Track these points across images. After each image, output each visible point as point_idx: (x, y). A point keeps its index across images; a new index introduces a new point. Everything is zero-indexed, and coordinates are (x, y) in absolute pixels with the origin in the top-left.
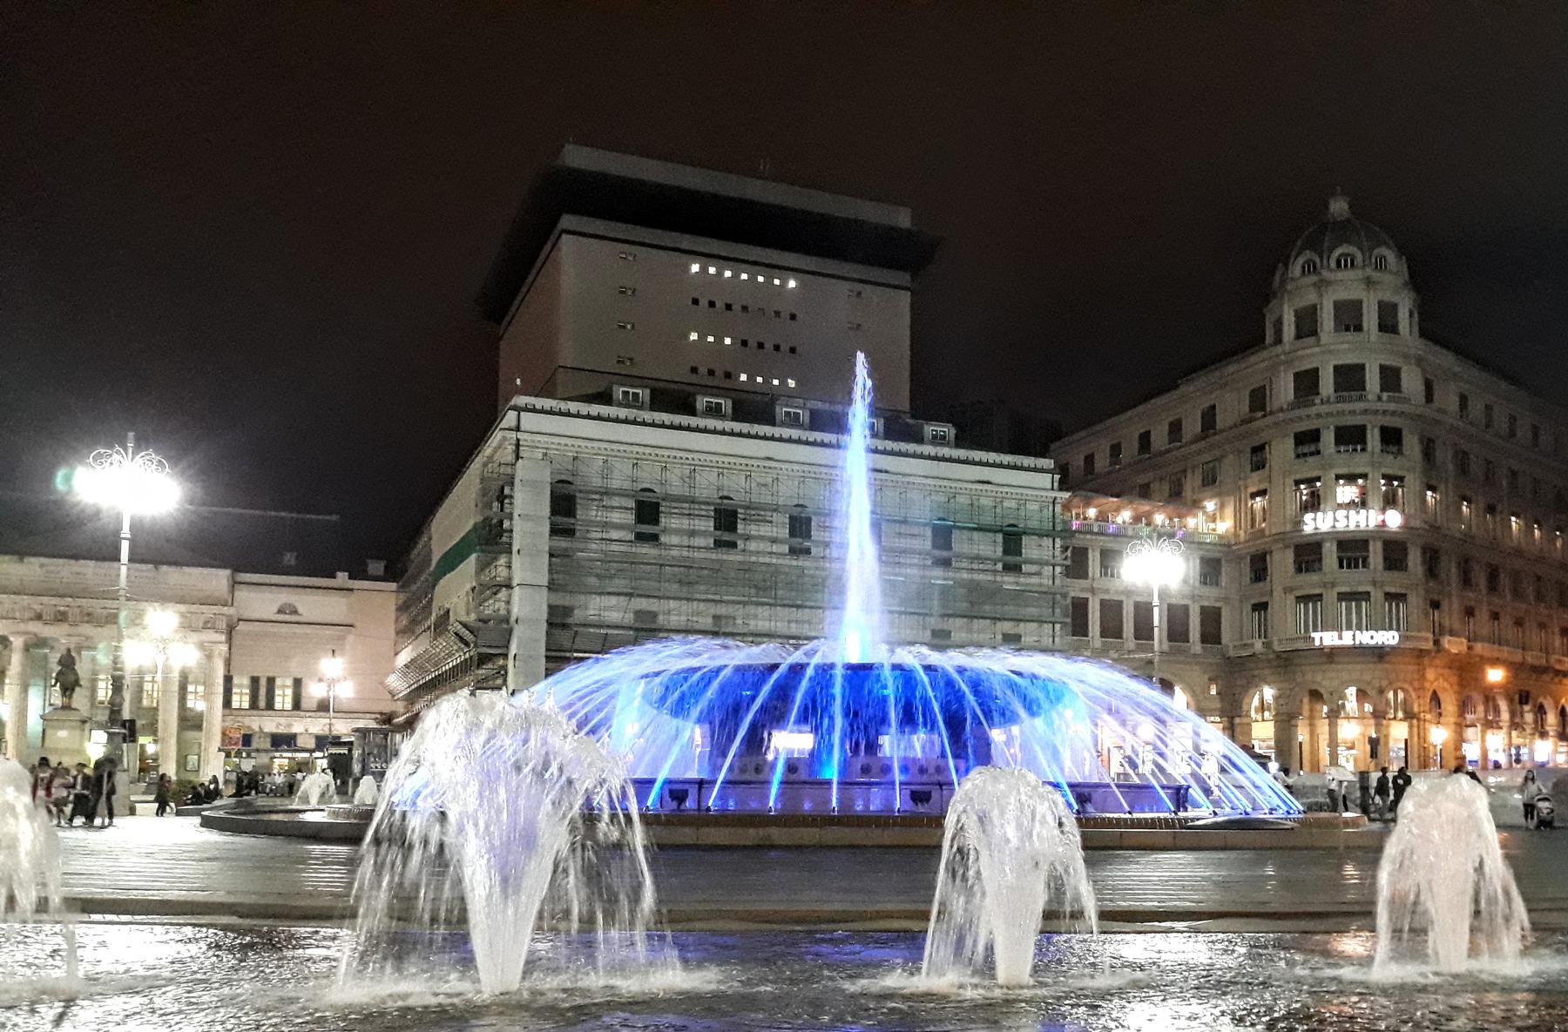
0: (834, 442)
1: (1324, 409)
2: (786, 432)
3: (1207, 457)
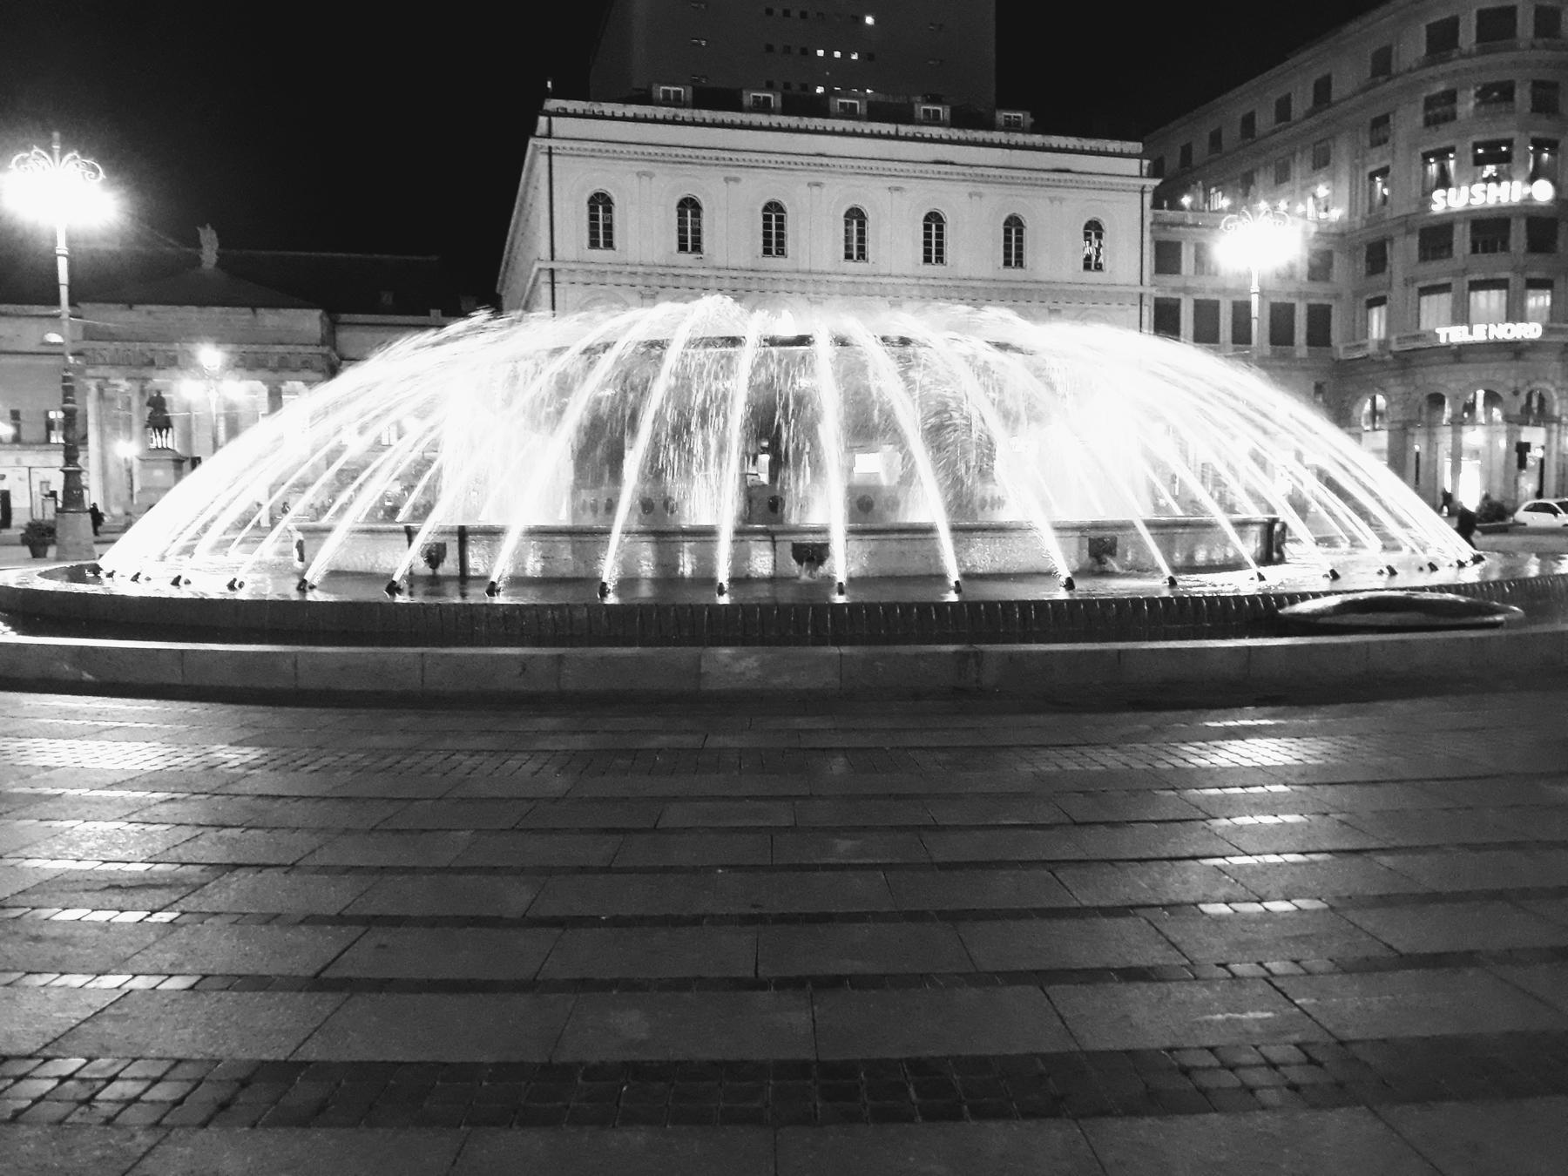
0: (893, 132)
1: (1465, 63)
2: (840, 125)
3: (1318, 135)
